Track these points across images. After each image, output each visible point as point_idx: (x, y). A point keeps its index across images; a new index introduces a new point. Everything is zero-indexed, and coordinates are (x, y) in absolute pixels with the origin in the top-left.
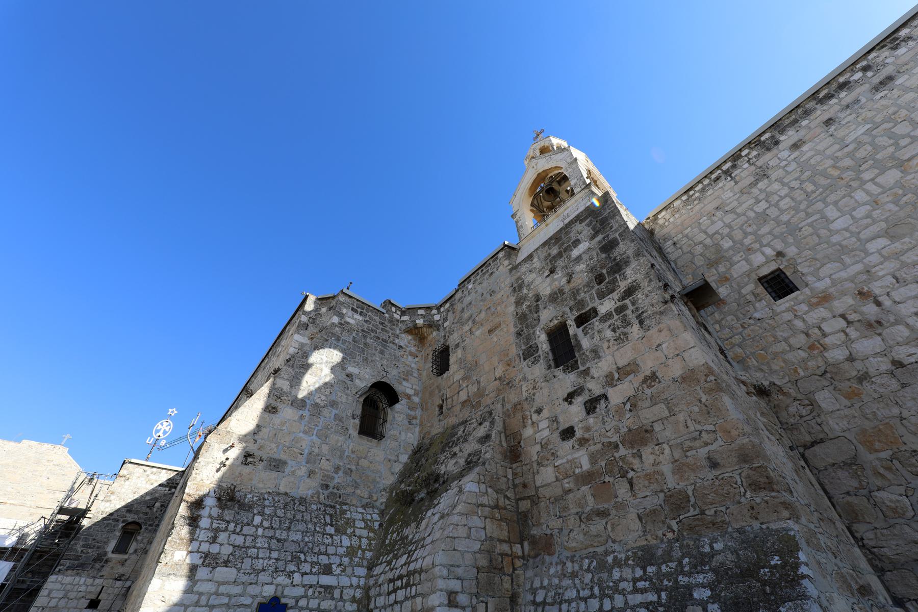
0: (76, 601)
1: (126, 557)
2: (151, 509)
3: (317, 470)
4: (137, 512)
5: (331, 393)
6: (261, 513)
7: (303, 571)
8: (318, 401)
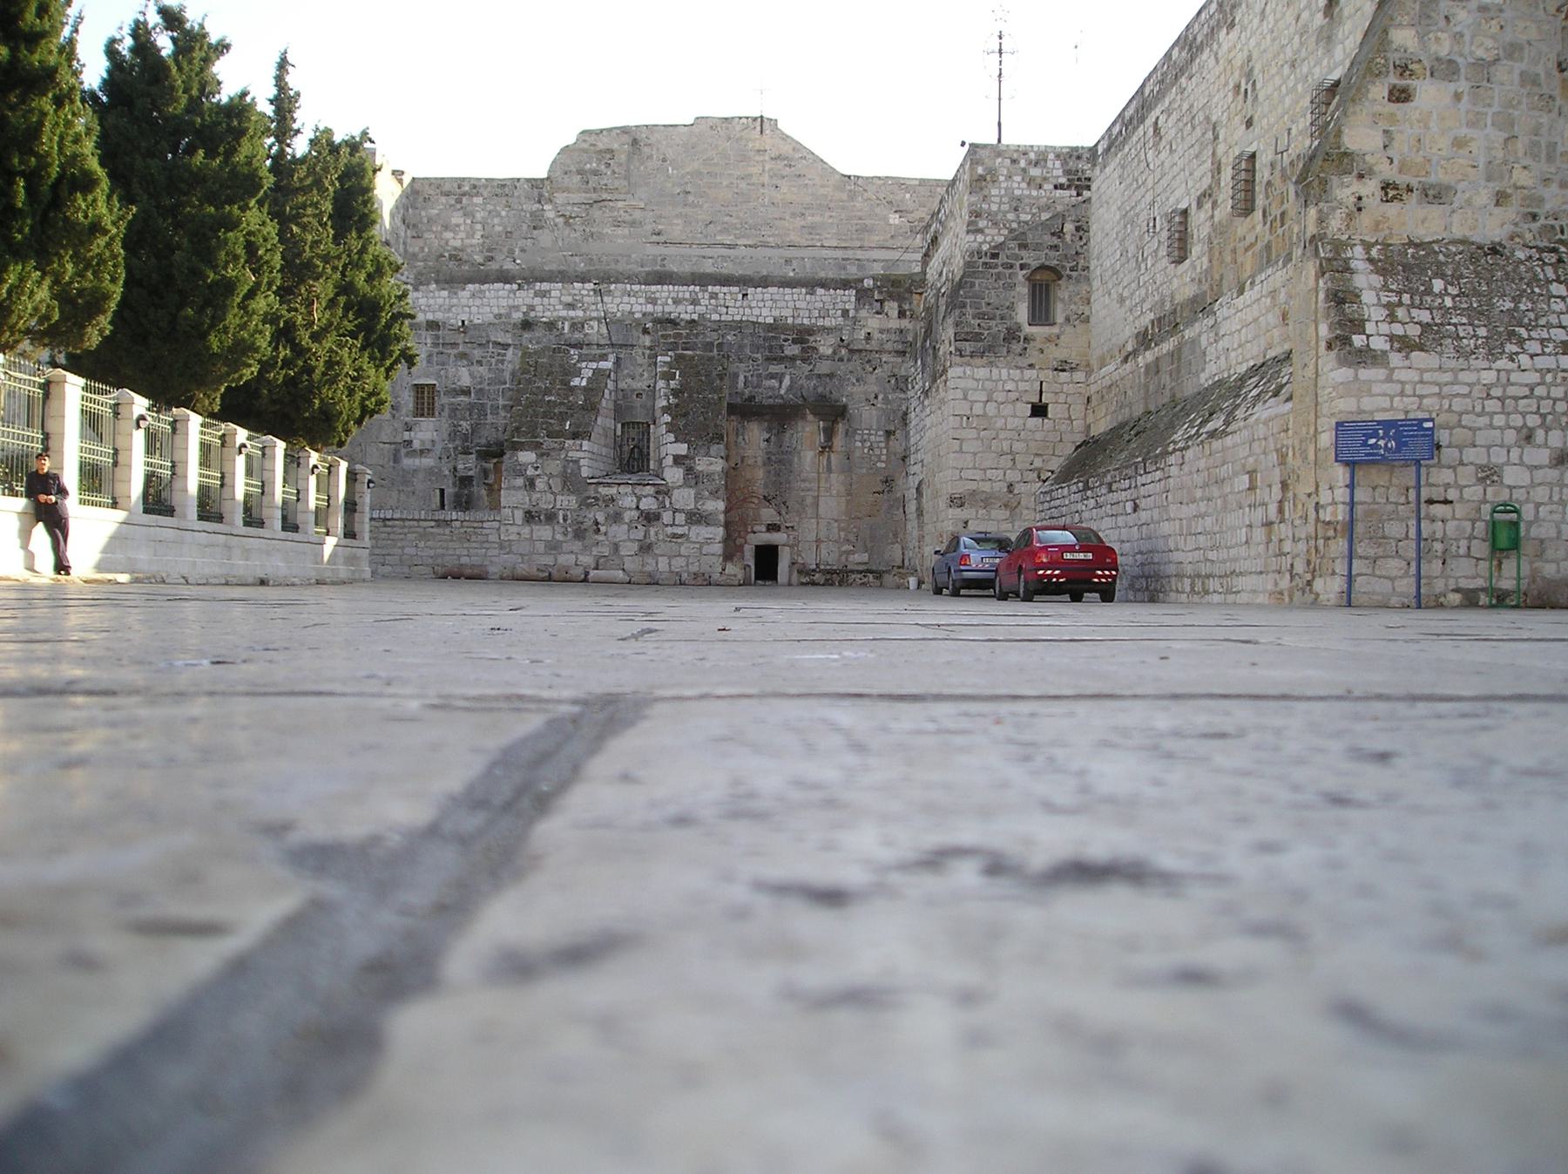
0: (1010, 406)
1: (1055, 330)
2: (1059, 237)
3: (1509, 191)
4: (1037, 247)
5: (1502, 27)
6: (1443, 276)
7: (1531, 352)
8: (1480, 53)
